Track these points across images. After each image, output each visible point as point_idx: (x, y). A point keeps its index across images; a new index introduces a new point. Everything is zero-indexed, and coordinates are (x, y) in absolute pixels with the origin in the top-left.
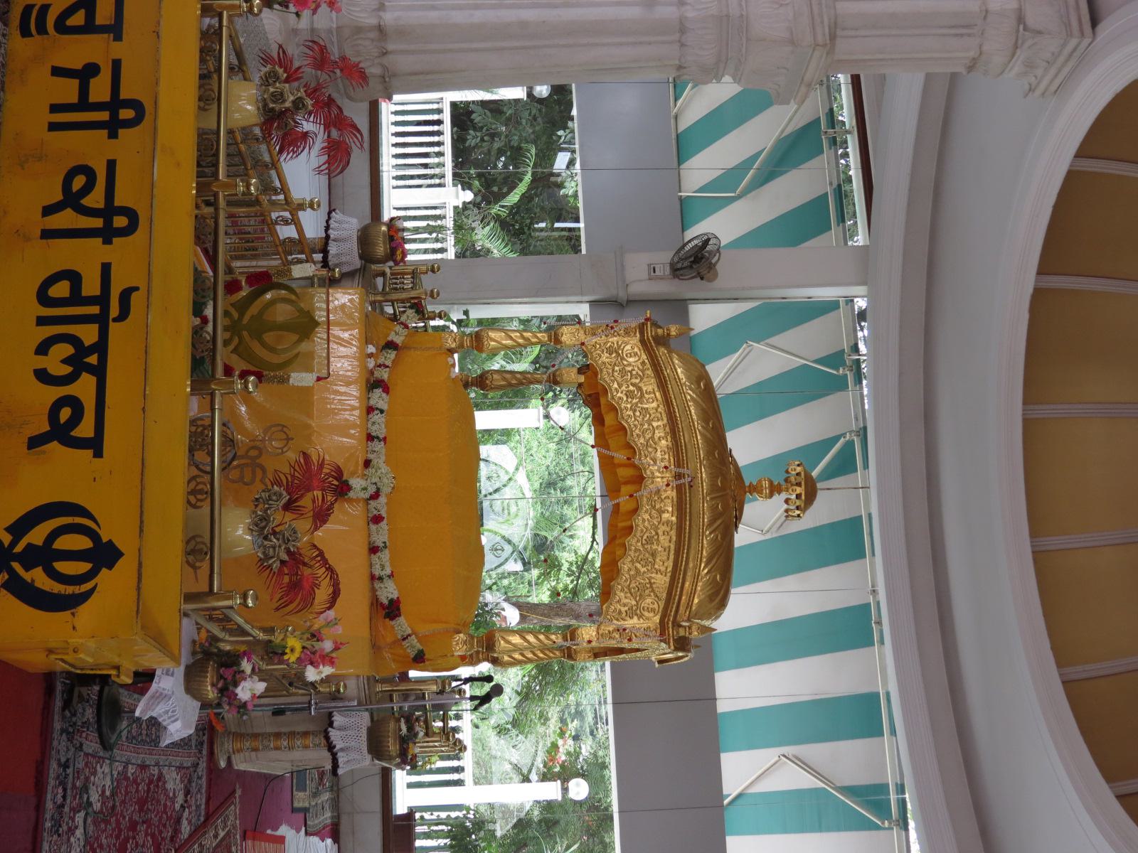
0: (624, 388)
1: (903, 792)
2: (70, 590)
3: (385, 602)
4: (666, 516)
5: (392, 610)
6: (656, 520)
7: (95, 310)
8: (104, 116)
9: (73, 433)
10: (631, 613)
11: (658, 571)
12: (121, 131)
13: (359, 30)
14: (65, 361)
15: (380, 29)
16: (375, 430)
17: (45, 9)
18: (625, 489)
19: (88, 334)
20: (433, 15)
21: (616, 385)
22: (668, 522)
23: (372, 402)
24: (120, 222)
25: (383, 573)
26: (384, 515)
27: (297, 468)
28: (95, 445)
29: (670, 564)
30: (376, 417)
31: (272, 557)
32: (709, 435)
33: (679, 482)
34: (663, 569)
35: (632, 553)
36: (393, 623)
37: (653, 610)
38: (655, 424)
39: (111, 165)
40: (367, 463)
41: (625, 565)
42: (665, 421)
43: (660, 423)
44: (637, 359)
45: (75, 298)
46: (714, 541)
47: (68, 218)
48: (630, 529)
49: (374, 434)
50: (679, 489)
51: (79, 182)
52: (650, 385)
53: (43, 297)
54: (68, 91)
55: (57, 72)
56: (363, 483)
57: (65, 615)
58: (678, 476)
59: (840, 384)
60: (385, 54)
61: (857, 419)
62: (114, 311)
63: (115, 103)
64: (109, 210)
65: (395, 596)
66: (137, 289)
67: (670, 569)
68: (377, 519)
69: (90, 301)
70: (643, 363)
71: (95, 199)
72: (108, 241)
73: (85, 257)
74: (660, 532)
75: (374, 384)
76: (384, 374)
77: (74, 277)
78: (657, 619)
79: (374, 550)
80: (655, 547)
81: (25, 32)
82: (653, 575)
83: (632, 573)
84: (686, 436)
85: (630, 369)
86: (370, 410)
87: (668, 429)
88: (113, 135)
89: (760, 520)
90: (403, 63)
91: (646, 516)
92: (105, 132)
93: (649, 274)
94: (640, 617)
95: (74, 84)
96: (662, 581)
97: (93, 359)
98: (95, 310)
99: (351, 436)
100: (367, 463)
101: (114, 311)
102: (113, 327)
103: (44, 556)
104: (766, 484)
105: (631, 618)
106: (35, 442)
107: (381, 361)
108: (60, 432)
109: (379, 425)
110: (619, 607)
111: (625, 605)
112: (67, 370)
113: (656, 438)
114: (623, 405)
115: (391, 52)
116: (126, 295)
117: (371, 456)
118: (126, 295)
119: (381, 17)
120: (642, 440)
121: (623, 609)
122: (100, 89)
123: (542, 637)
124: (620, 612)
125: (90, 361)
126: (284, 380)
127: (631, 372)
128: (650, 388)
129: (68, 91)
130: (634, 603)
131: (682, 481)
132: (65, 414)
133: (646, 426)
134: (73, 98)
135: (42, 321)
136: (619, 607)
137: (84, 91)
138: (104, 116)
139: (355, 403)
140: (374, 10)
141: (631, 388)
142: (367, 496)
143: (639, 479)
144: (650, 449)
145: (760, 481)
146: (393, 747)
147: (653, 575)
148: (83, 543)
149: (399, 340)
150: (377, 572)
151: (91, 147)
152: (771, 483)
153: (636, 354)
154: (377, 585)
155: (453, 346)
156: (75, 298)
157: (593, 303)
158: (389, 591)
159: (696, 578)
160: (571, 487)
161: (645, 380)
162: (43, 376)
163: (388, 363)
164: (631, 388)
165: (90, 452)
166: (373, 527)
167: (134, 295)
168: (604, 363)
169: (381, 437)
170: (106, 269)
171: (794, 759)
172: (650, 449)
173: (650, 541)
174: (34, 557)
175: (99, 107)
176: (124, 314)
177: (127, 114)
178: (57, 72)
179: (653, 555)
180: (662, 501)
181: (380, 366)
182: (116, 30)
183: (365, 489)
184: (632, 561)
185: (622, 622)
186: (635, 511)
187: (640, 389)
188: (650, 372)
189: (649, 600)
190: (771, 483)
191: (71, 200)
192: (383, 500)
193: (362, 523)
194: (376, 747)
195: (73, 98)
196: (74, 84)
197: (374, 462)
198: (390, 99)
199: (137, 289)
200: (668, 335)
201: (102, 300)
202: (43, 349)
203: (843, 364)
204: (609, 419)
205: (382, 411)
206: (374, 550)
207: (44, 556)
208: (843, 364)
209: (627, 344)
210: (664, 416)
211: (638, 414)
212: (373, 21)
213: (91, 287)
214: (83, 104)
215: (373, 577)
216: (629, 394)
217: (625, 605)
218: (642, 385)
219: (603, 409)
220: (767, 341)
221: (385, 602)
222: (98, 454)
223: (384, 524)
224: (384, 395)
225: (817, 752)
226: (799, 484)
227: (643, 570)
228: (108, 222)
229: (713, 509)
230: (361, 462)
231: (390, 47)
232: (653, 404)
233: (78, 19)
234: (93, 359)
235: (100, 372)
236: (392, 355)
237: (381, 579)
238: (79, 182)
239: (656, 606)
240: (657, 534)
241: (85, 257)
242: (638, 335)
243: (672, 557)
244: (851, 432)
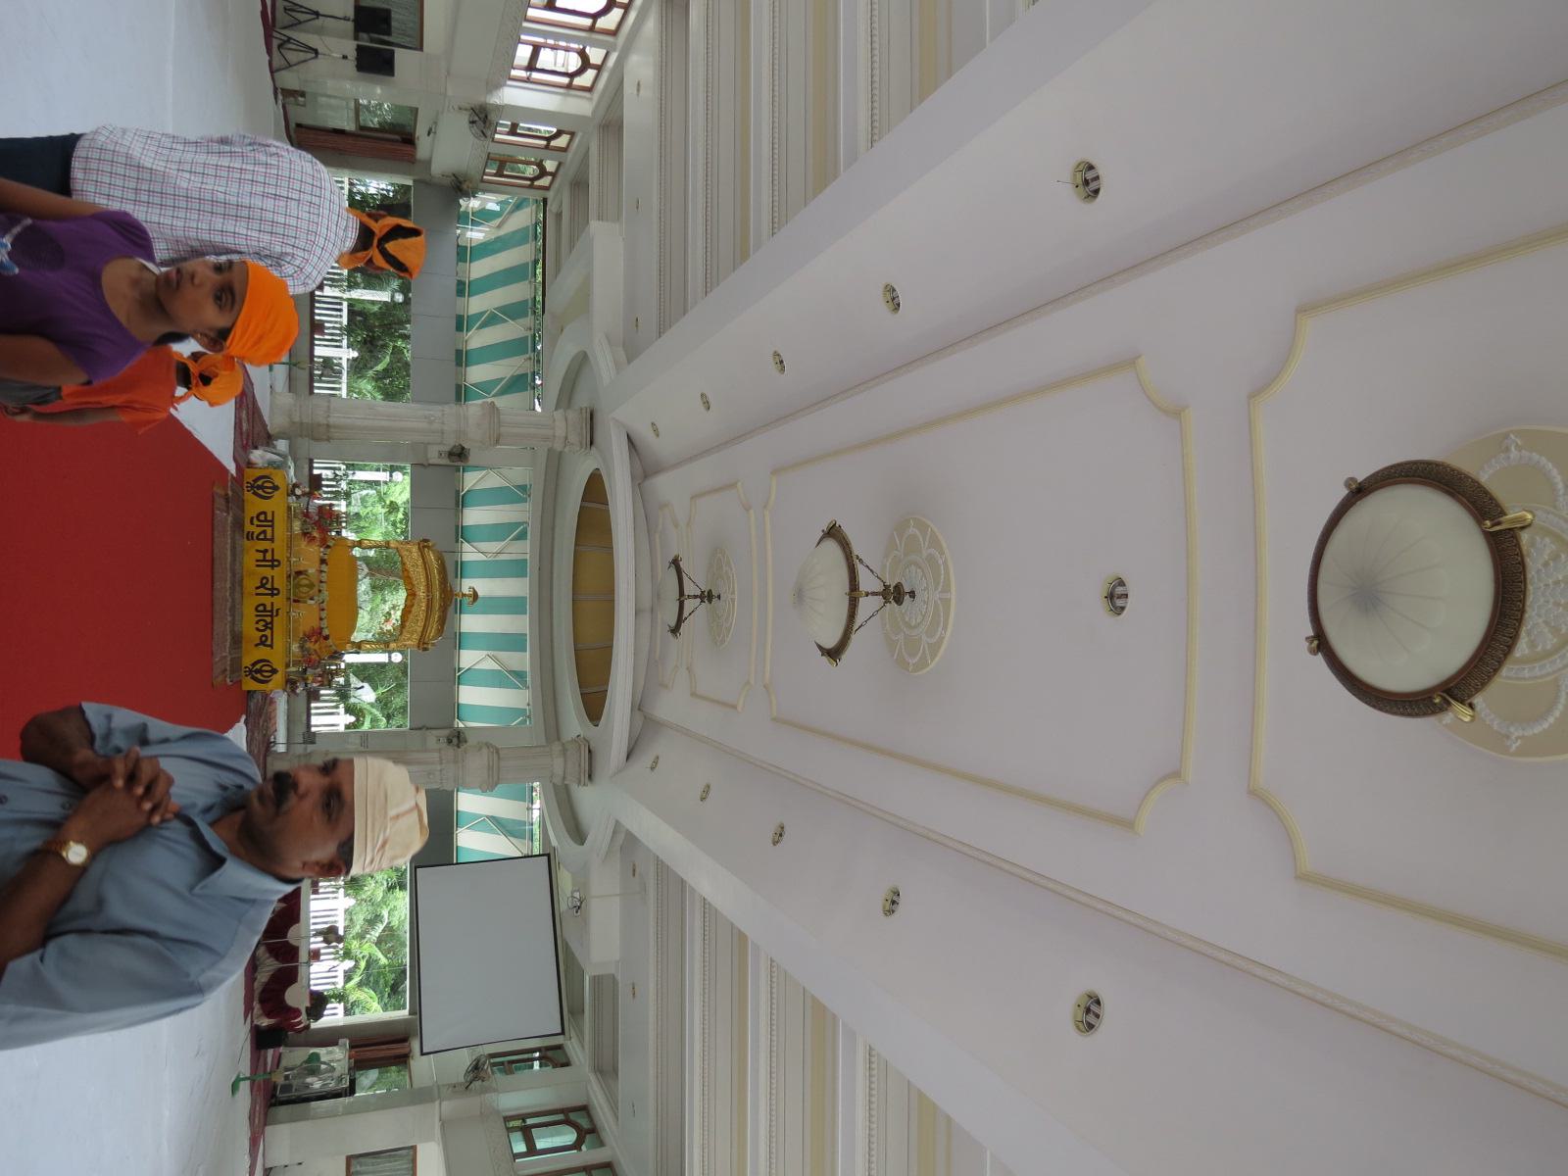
17: (253, 533)
19: (269, 619)
24: (275, 592)
28: (271, 646)
39: (273, 577)
45: (265, 610)
47: (262, 591)
51: (264, 581)
53: (256, 609)
54: (260, 556)
55: (257, 551)
63: (273, 560)
64: (273, 589)
71: (269, 586)
73: (267, 600)
81: (248, 539)
88: (273, 569)
102: (275, 618)
103: (259, 671)
106: (256, 645)
108: (262, 643)
116: (277, 610)
118: (277, 610)
122: (269, 556)
125: (269, 626)
129: (260, 556)
132: (264, 639)
134: (262, 558)
135: (257, 616)
137: (264, 556)
151: (267, 572)
162: (257, 629)
170: (272, 604)
174: (257, 671)
175: (268, 561)
176: (277, 615)
177: (276, 563)
178: (257, 551)
182: (272, 540)
191: (262, 586)
195: (262, 558)
201: (272, 611)
202: (257, 623)
207: (259, 671)
213: (269, 608)
214: (264, 560)
222: (272, 648)
233: (262, 536)
235: (272, 629)
238: (264, 581)
241: (267, 600)
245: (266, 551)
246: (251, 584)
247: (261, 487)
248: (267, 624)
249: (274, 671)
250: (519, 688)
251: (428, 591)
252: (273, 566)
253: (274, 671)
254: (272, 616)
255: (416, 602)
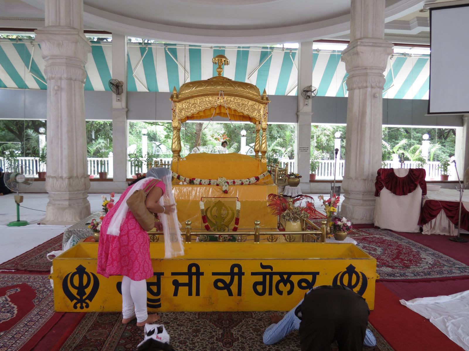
0: (193, 109)
1: (268, 47)
2: (361, 280)
3: (256, 181)
4: (232, 100)
5: (257, 179)
6: (234, 103)
7: (268, 277)
8: (194, 278)
9: (311, 282)
10: (259, 112)
11: (248, 103)
12: (201, 271)
13: (70, 185)
14: (285, 285)
15: (70, 178)
16: (207, 182)
18: (223, 111)
19: (276, 278)
20: (64, 161)
21: (192, 111)
22: (234, 99)
23: (198, 183)
24: (236, 270)
25: (248, 181)
26: (233, 180)
27: (274, 208)
29: (246, 100)
30: (203, 182)
31: (307, 216)
32: (206, 85)
33: (223, 95)
34: (247, 102)
35: (242, 111)
36: (260, 179)
37: (259, 106)
38: (204, 100)
39: (214, 274)
40: (218, 185)
41: (246, 113)
42: (204, 97)
43: (204, 99)
44: (184, 104)
45: (263, 283)
46: (238, 86)
47: (234, 288)
48: (235, 110)
49: (208, 183)
50: (225, 95)
51: (220, 284)
52: (192, 101)
53: (262, 294)
54: (183, 291)
55: (176, 294)
56: (224, 186)
57: (368, 280)
58: (221, 95)
59: (150, 49)
60: (77, 177)
61: (162, 46)
62: (269, 270)
63: (189, 274)
64: (232, 274)
65: (254, 178)
66: (261, 264)
67: (247, 100)
68: (234, 182)
69: (264, 279)
70: (185, 102)
71: (227, 279)
72: (243, 274)
73: (248, 281)
74: (236, 102)
75: (191, 182)
76: (188, 179)
77: (256, 284)
78: (261, 105)
79: (242, 184)
80: (241, 104)
81: (159, 306)
82: (249, 105)
83: (248, 111)
84: (207, 91)
85: (187, 107)
86: (200, 184)
87: (206, 97)
89: (229, 72)
90: (80, 171)
91: (232, 105)
92: (201, 277)
93: (120, 101)
94: (260, 110)
95: (180, 288)
96: (251, 103)
97: (285, 277)
98: (268, 277)
99: (209, 189)
100: (218, 185)
101: (269, 270)
102: (274, 270)
104: (219, 70)
105: (260, 112)
107: (183, 180)
109: (205, 181)
110: (257, 116)
111: (257, 114)
112: (288, 285)
113: (208, 100)
114: (198, 109)
115: (77, 174)
116: (263, 267)
117: (215, 184)
118: (263, 267)
119: (65, 178)
120: (209, 105)
121: (258, 114)
122: (184, 279)
123: (263, 138)
124: (258, 115)
125: (285, 277)
126: (238, 211)
127: (188, 106)
128: (193, 101)
129: (183, 291)
130: (256, 111)
131: (223, 94)
132: (304, 284)
133: (205, 103)
134: (187, 288)
135: (270, 293)
136: (257, 116)
138: (194, 278)
139: (198, 189)
140: (62, 180)
141: (193, 106)
142: (228, 185)
143: (220, 107)
144: (212, 102)
145: (218, 71)
146: (297, 180)
147: (249, 105)
148: (346, 277)
149: (177, 175)
150: (248, 183)
151: (207, 281)
152: (218, 68)
153: (182, 104)
154: (251, 183)
155: (177, 159)
156: (263, 283)
157: (127, 119)
158: (253, 180)
159: (249, 93)
160: (139, 131)
161: (190, 102)
162: (290, 292)
163: (184, 178)
164: (193, 106)
165: (317, 276)
166: (236, 184)
167: (264, 264)
168: (185, 114)
169: (209, 181)
170: (253, 274)
171: (250, 76)
172: (212, 102)
173: (239, 105)
175: (190, 279)
176: (271, 267)
177: (194, 270)
178: (176, 294)
179: (243, 104)
180: (227, 100)
181: (185, 181)
183: (226, 186)
184: (245, 110)
185: (261, 115)
186: (229, 108)
187: (193, 104)
188: (188, 100)
189: (256, 107)
190: (218, 68)
191: (227, 287)
192: (228, 181)
193: (235, 187)
194: (296, 184)
195: (187, 288)
196: (180, 288)
197: (218, 183)
198: (89, 175)
199: (261, 264)
200: (176, 94)
201: (264, 275)
202: (280, 293)
203: (145, 48)
204: (202, 114)
205: (201, 180)
206: (242, 184)
208: (145, 48)
209: (179, 107)
210: (202, 97)
211: (201, 105)
212: (67, 181)
213: (260, 278)
214: (189, 285)
215: (249, 184)
216: (195, 107)
217: (257, 114)
218: (192, 103)
219: (198, 115)
220: (133, 69)
221: (256, 181)
222: (318, 273)
223: (236, 181)
224: (196, 180)
225: (249, 69)
226: (221, 60)
227: (247, 108)
228: (236, 274)
229: (229, 86)
230: (217, 187)
231: (75, 175)
232: (198, 100)
234: (285, 277)
235: (290, 274)
236: (181, 177)
237: (250, 182)
238: (220, 284)
239: (257, 105)
240: (237, 103)
242: (176, 103)
243: (244, 99)
244: (165, 48)
245: (176, 284)
246: (223, 302)
247: (81, 289)
248: (282, 280)
249: (351, 270)
250: (271, 57)
251: (218, 95)
252: (199, 274)
253: (351, 270)
254: (271, 274)
255: (226, 106)
